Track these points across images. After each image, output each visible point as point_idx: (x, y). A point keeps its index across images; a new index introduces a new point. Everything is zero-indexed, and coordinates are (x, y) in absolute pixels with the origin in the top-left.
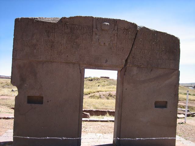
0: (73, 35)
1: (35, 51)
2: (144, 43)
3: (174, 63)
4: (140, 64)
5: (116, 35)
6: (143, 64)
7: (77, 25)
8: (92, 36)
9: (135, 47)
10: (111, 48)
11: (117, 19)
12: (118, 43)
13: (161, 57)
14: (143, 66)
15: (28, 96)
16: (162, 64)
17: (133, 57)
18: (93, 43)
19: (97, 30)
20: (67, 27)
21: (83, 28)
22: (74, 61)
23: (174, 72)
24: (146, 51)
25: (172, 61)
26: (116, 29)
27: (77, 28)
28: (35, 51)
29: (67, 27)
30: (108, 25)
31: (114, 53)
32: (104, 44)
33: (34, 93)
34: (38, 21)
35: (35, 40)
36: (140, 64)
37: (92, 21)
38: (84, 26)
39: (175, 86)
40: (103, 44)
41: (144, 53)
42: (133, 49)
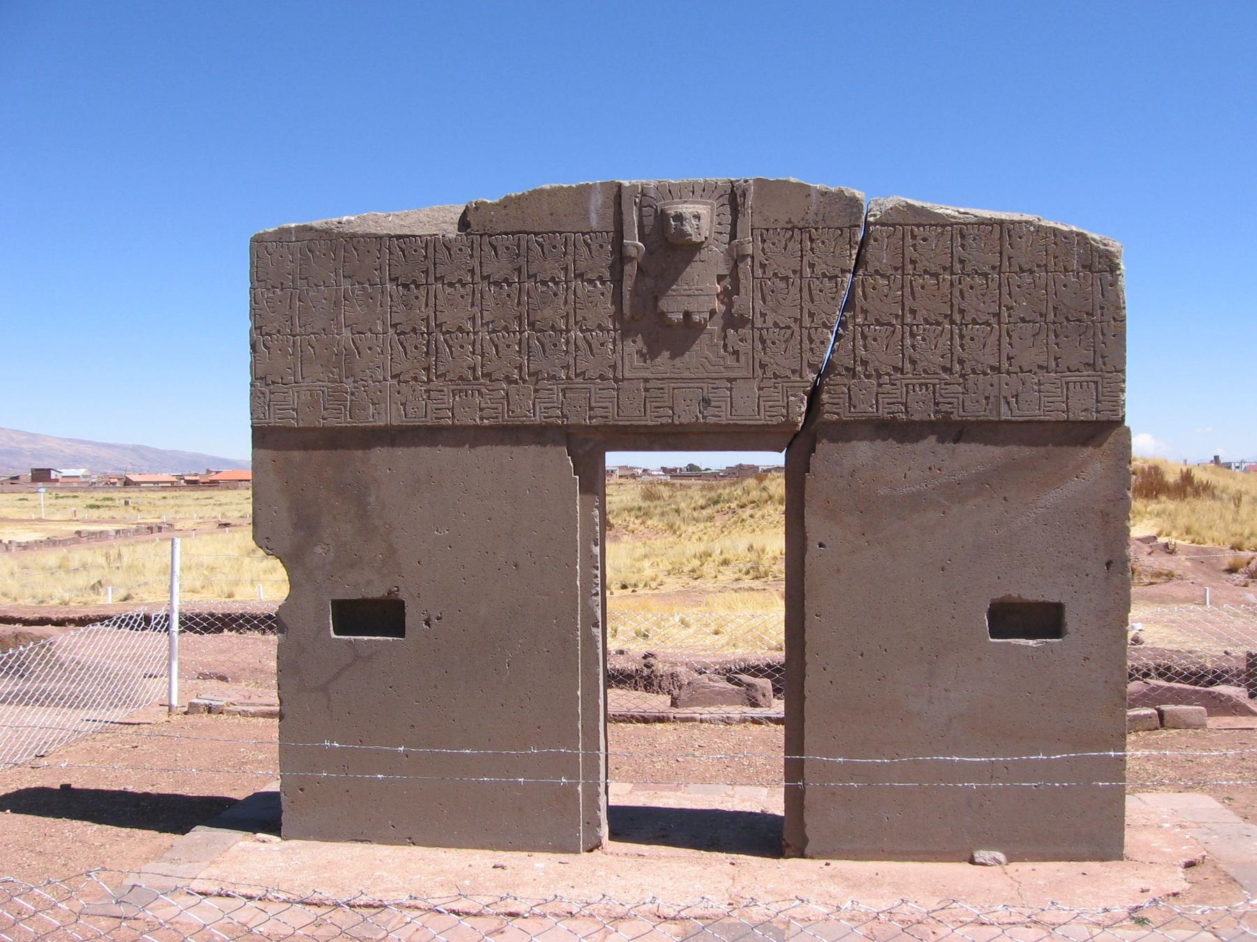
1: (349, 385)
3: (1092, 386)
4: (895, 408)
6: (905, 405)
7: (540, 233)
11: (746, 181)
15: (334, 602)
16: (1016, 396)
20: (495, 248)
21: (571, 248)
30: (697, 217)
31: (742, 358)
32: (687, 315)
34: (353, 236)
36: (895, 408)
39: (1105, 515)
40: (677, 317)
41: (913, 346)
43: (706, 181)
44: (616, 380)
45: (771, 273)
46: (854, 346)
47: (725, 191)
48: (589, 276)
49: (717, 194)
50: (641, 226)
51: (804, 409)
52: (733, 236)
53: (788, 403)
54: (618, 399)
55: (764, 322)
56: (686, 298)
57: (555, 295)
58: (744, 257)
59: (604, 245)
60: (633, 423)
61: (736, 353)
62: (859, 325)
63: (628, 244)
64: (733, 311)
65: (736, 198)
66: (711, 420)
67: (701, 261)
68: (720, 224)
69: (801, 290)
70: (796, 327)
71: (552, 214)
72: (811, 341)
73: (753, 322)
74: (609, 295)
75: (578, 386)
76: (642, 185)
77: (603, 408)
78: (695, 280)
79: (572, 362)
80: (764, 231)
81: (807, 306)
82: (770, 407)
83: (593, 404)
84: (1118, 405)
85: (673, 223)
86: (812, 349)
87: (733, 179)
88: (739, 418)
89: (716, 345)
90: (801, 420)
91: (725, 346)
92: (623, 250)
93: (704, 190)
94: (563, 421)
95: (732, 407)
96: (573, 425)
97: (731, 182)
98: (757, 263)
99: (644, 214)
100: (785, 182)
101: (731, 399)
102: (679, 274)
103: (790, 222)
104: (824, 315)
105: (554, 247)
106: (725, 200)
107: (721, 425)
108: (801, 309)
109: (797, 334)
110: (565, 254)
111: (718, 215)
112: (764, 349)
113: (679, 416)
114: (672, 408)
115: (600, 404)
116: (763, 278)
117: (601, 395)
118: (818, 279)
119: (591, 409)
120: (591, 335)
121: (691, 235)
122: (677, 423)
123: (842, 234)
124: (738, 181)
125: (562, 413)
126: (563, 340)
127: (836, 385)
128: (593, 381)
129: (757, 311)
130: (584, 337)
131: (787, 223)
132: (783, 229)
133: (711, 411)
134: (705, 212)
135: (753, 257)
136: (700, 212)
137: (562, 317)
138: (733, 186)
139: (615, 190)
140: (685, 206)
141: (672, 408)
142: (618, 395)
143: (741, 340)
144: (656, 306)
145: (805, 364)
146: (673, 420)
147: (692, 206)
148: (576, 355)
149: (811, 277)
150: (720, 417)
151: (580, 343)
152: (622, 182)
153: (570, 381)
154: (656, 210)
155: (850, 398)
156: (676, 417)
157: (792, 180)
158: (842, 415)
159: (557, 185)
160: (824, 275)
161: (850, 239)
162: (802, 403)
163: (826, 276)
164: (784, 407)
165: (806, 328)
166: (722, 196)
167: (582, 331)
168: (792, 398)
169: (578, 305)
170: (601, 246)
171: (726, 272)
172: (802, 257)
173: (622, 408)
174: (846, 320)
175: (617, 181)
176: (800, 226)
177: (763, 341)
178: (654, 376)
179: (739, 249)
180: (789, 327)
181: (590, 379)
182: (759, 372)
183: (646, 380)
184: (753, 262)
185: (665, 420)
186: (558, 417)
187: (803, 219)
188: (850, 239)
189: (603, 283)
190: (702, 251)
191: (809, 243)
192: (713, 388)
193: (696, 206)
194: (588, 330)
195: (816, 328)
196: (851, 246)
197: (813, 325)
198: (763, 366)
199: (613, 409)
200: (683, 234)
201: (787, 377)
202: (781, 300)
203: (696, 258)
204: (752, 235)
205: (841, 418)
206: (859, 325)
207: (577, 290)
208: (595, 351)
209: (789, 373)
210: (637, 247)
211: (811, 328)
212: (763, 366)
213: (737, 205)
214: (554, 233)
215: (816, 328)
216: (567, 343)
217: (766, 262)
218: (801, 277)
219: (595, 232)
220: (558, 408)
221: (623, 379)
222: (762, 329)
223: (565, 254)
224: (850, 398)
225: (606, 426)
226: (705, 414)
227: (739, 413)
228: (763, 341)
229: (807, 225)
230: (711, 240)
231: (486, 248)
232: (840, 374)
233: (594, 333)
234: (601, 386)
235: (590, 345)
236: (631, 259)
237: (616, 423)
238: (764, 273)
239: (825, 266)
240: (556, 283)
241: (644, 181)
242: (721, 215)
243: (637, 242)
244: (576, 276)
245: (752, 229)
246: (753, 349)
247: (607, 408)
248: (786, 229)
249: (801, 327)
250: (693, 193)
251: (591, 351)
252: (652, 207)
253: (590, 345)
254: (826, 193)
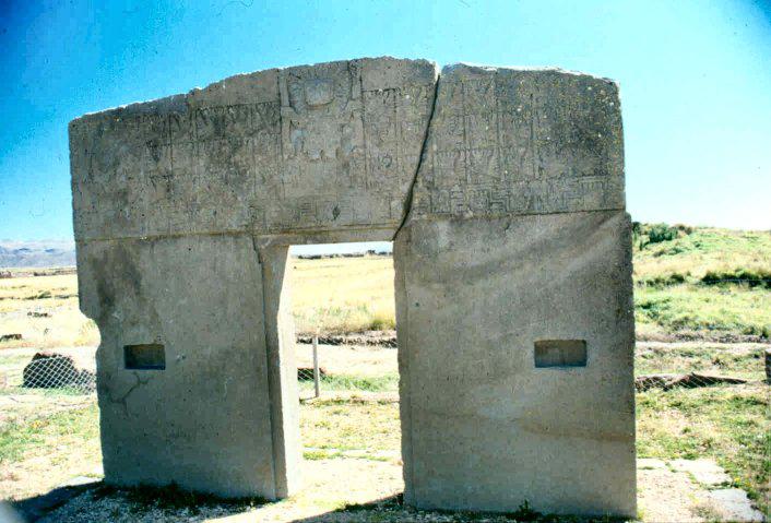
0: (223, 141)
1: (126, 209)
2: (467, 127)
5: (357, 115)
8: (280, 133)
9: (435, 147)
10: (346, 166)
11: (356, 61)
12: (368, 143)
13: (541, 169)
14: (471, 213)
17: (431, 186)
18: (286, 157)
19: (292, 110)
20: (204, 118)
22: (235, 228)
23: (603, 221)
24: (478, 156)
25: (586, 180)
26: (356, 93)
27: (232, 115)
28: (126, 209)
29: (204, 118)
31: (359, 180)
33: (141, 336)
35: (123, 178)
37: (276, 85)
38: (254, 107)
42: (429, 156)
84: (621, 197)
231: (200, 119)
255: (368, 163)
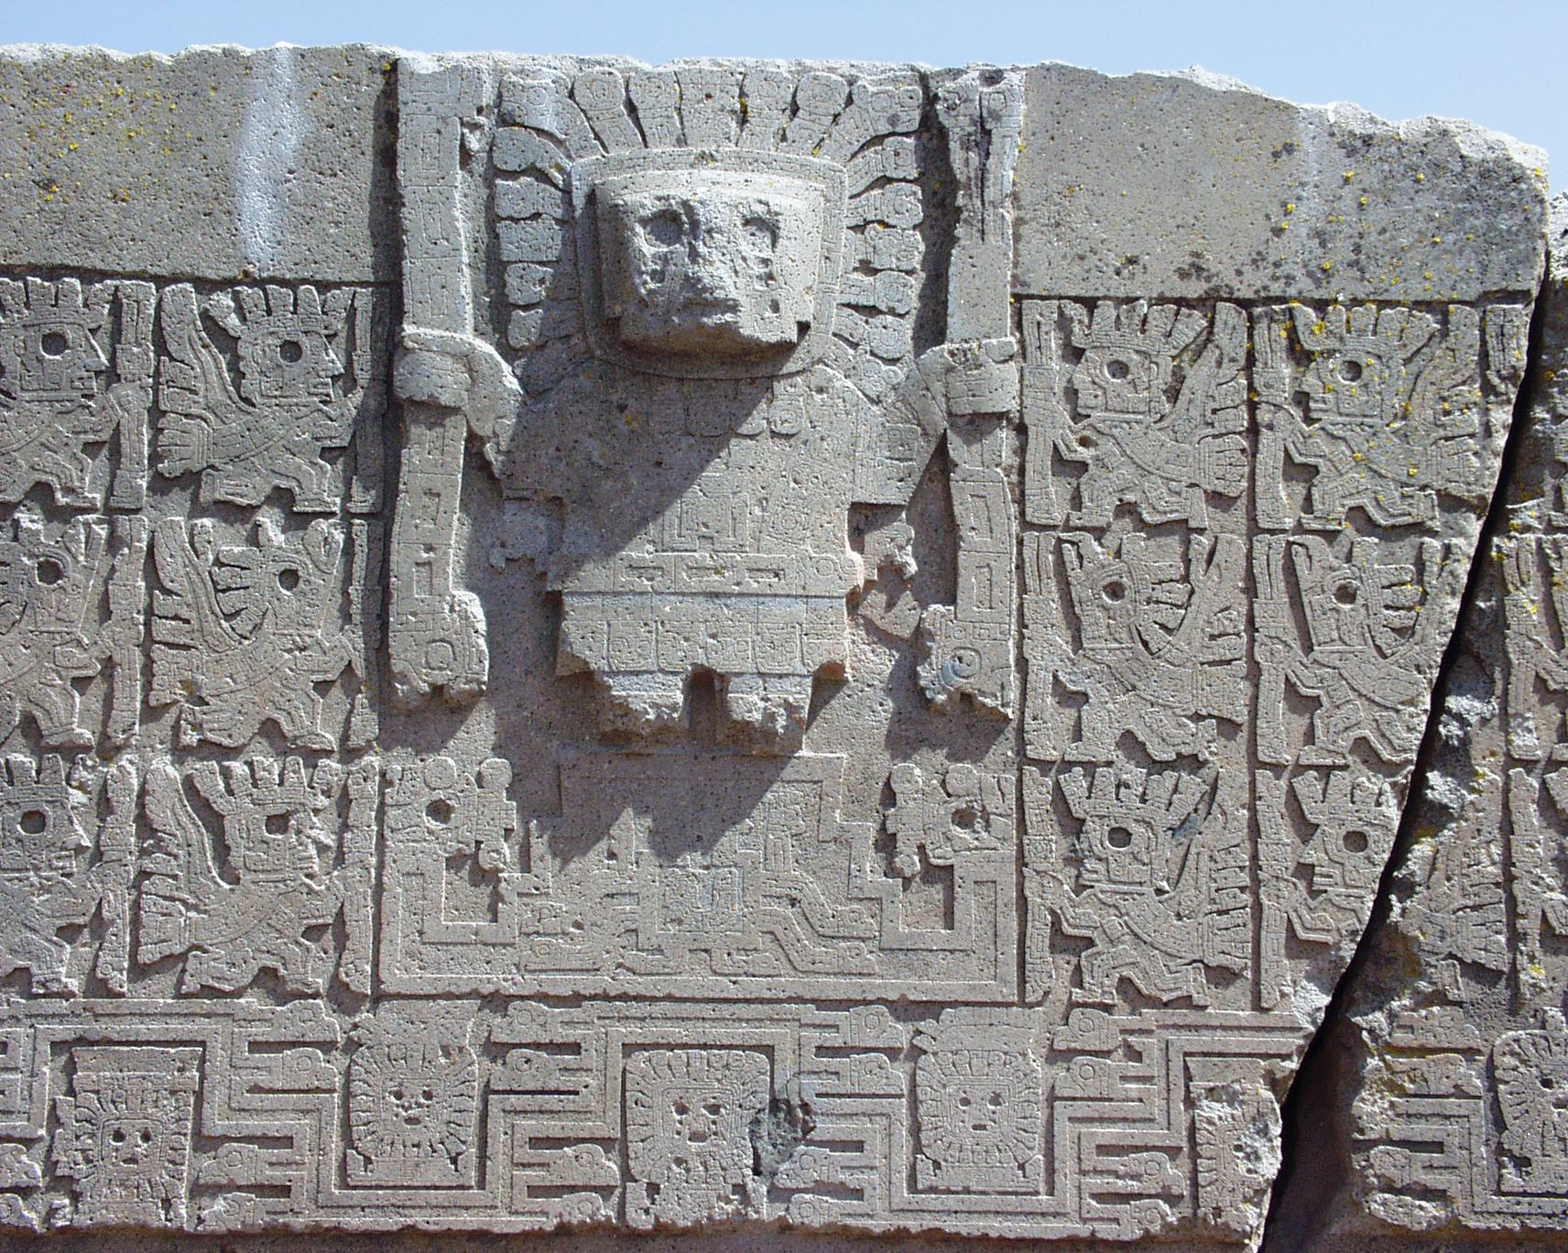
11: (992, 78)
21: (138, 357)
30: (765, 225)
31: (968, 906)
43: (803, 70)
44: (342, 997)
45: (1110, 503)
46: (1507, 862)
47: (893, 120)
48: (218, 489)
49: (852, 130)
50: (494, 266)
51: (1270, 1165)
52: (931, 328)
53: (1193, 1130)
54: (348, 1095)
55: (1077, 735)
56: (700, 606)
57: (51, 571)
58: (978, 424)
59: (305, 342)
60: (419, 1219)
61: (940, 875)
62: (1529, 765)
63: (425, 345)
64: (925, 674)
65: (945, 150)
66: (814, 1211)
67: (774, 434)
68: (867, 268)
69: (1251, 590)
70: (1227, 761)
71: (47, 185)
72: (1306, 829)
73: (1021, 730)
74: (324, 582)
75: (142, 1028)
76: (498, 72)
77: (265, 1141)
78: (749, 526)
79: (117, 906)
80: (1076, 311)
81: (1280, 661)
82: (1103, 1149)
83: (217, 1124)
85: (648, 250)
86: (1305, 871)
87: (926, 66)
88: (951, 1202)
89: (843, 840)
90: (1254, 1217)
91: (887, 843)
92: (401, 371)
93: (795, 109)
94: (52, 1212)
95: (918, 1148)
96: (104, 1233)
97: (923, 79)
98: (1039, 457)
99: (504, 208)
100: (1175, 85)
101: (914, 1103)
102: (673, 492)
103: (1196, 270)
104: (1362, 712)
105: (55, 342)
106: (904, 158)
107: (865, 1236)
108: (1254, 673)
109: (1232, 797)
110: (111, 375)
111: (859, 228)
112: (1075, 860)
113: (653, 1189)
114: (616, 1145)
115: (254, 1125)
116: (1068, 528)
117: (262, 1078)
118: (1330, 536)
119: (204, 1142)
120: (226, 774)
121: (734, 307)
122: (643, 1222)
123: (1445, 334)
124: (955, 74)
125: (50, 1166)
126: (77, 797)
127: (1422, 1051)
128: (220, 1005)
129: (1041, 679)
130: (189, 782)
131: (1183, 275)
132: (1162, 300)
133: (813, 1164)
134: (800, 205)
135: (1021, 429)
136: (777, 202)
137: (81, 683)
138: (931, 99)
139: (370, 88)
140: (706, 173)
141: (616, 1145)
142: (347, 1074)
143: (963, 819)
144: (553, 640)
145: (1274, 940)
146: (622, 1213)
147: (732, 176)
148: (144, 874)
149: (1300, 528)
150: (858, 1194)
151: (159, 814)
152: (401, 53)
153: (103, 1004)
154: (567, 192)
155: (1499, 1123)
156: (637, 1193)
157: (1207, 78)
158: (1460, 1205)
159: (79, 50)
160: (1361, 519)
161: (1484, 356)
162: (1264, 1132)
163: (1369, 526)
164: (1173, 1152)
165: (1277, 768)
166: (878, 140)
167: (180, 753)
168: (1213, 1110)
169: (163, 629)
170: (292, 350)
171: (894, 494)
172: (1253, 430)
173: (366, 1144)
174: (1466, 741)
175: (375, 49)
176: (1247, 293)
177: (1074, 826)
178: (528, 984)
179: (958, 385)
180: (1194, 763)
181: (209, 992)
182: (1052, 973)
183: (496, 1001)
184: (1022, 451)
185: (579, 1209)
186: (25, 1191)
187: (1258, 259)
188: (1484, 356)
189: (297, 521)
190: (779, 387)
191: (1287, 370)
192: (821, 1050)
193: (760, 179)
194: (207, 749)
195: (1326, 772)
196: (1488, 388)
197: (1311, 756)
198: (1067, 943)
199: (322, 1150)
200: (699, 299)
201: (1187, 1002)
202: (1156, 638)
203: (756, 422)
204: (1019, 326)
205: (1454, 1221)
206: (1529, 765)
207: (162, 556)
208: (235, 858)
209: (1194, 984)
210: (467, 360)
211: (1300, 769)
212: (1067, 943)
213: (951, 184)
214: (54, 272)
215: (1326, 772)
216: (104, 805)
217: (1084, 453)
218: (1254, 529)
219: (260, 283)
220: (29, 1142)
221: (378, 998)
222: (1067, 766)
223: (111, 375)
224: (1499, 1123)
225: (278, 1235)
226: (783, 1181)
227: (951, 1176)
228: (1074, 826)
229: (1276, 289)
230: (817, 343)
232: (1440, 998)
233: (238, 767)
234: (260, 1032)
235: (213, 820)
236: (437, 413)
237: (328, 1220)
238: (1076, 501)
239: (1363, 479)
240: (57, 514)
241: (510, 57)
242: (871, 231)
243: (467, 336)
244: (161, 484)
245: (1018, 298)
246: (1021, 861)
247: (287, 1141)
248: (1180, 302)
249: (1255, 763)
250: (743, 121)
251: (222, 851)
252: (542, 176)
253: (213, 820)
254: (1367, 141)
255: (1038, 791)
